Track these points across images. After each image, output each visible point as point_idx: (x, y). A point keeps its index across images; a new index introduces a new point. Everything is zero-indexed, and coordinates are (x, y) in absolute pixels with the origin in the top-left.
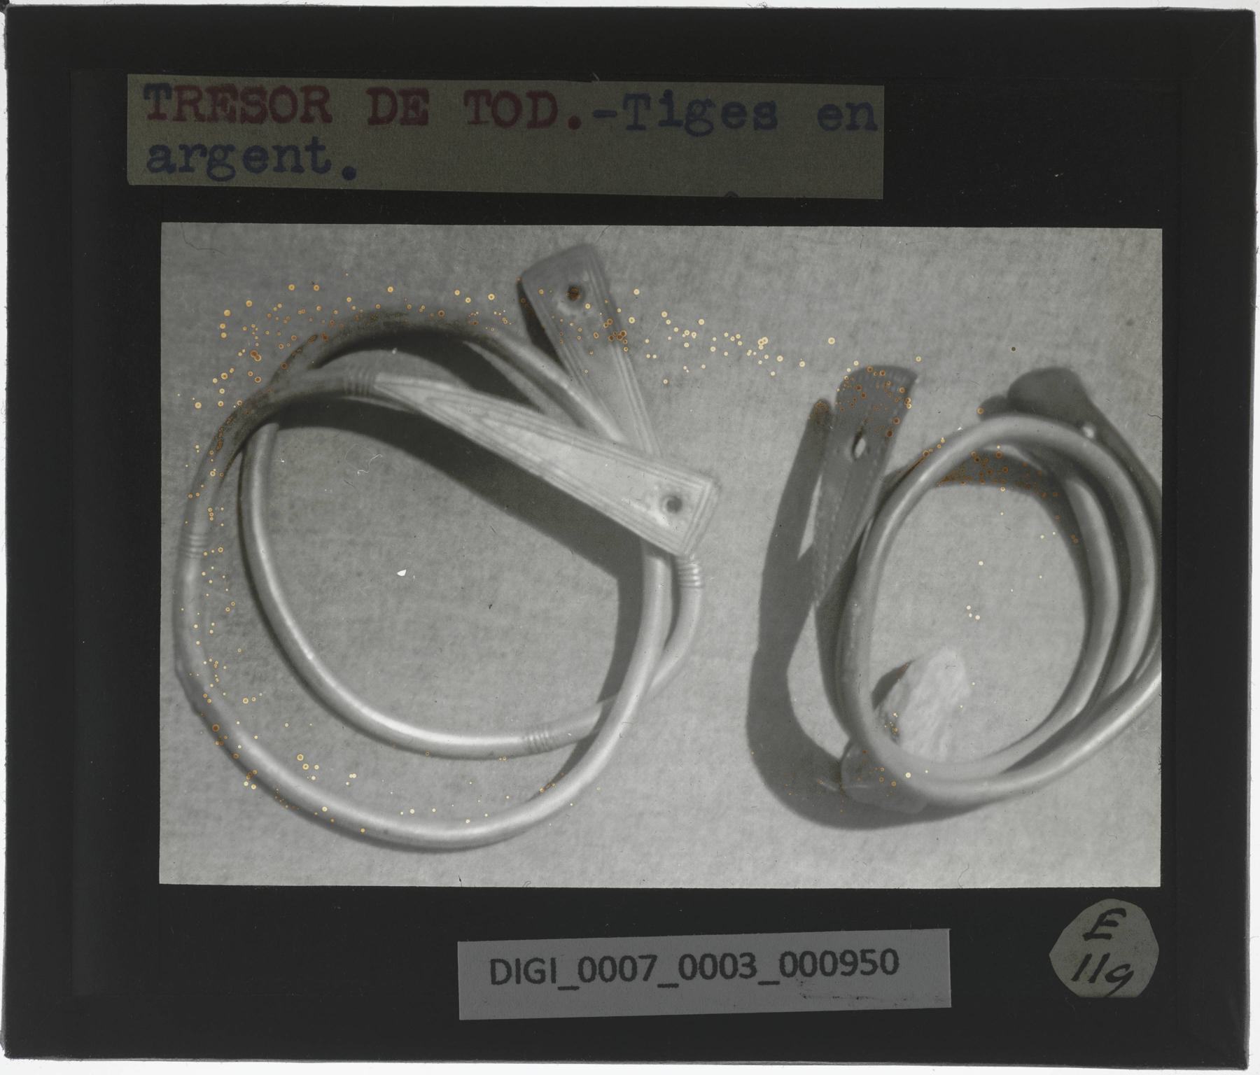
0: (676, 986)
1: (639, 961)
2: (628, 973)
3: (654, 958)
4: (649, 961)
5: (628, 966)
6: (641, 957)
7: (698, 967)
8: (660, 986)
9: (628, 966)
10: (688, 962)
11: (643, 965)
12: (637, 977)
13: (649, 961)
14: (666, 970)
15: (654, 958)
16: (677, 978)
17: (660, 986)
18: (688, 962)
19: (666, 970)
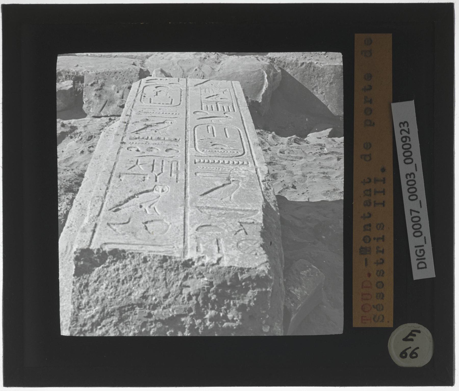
0: (420, 201)
1: (413, 216)
2: (416, 219)
3: (411, 210)
4: (412, 212)
5: (414, 219)
6: (411, 215)
7: (413, 194)
8: (421, 207)
9: (414, 219)
10: (412, 198)
11: (414, 214)
12: (419, 216)
13: (412, 212)
14: (415, 205)
15: (411, 210)
16: (418, 200)
17: (421, 207)
18: (412, 198)
19: (415, 205)
